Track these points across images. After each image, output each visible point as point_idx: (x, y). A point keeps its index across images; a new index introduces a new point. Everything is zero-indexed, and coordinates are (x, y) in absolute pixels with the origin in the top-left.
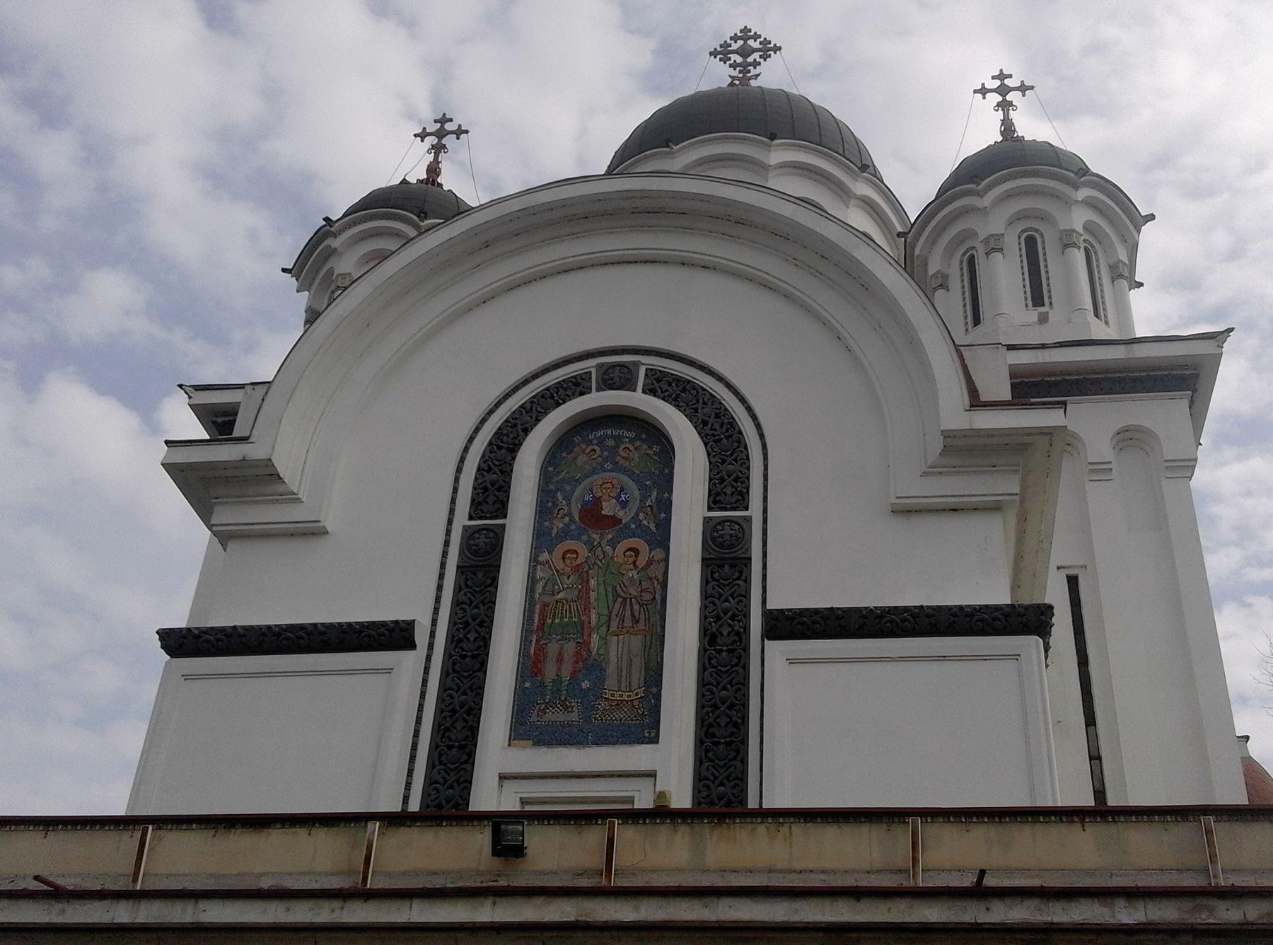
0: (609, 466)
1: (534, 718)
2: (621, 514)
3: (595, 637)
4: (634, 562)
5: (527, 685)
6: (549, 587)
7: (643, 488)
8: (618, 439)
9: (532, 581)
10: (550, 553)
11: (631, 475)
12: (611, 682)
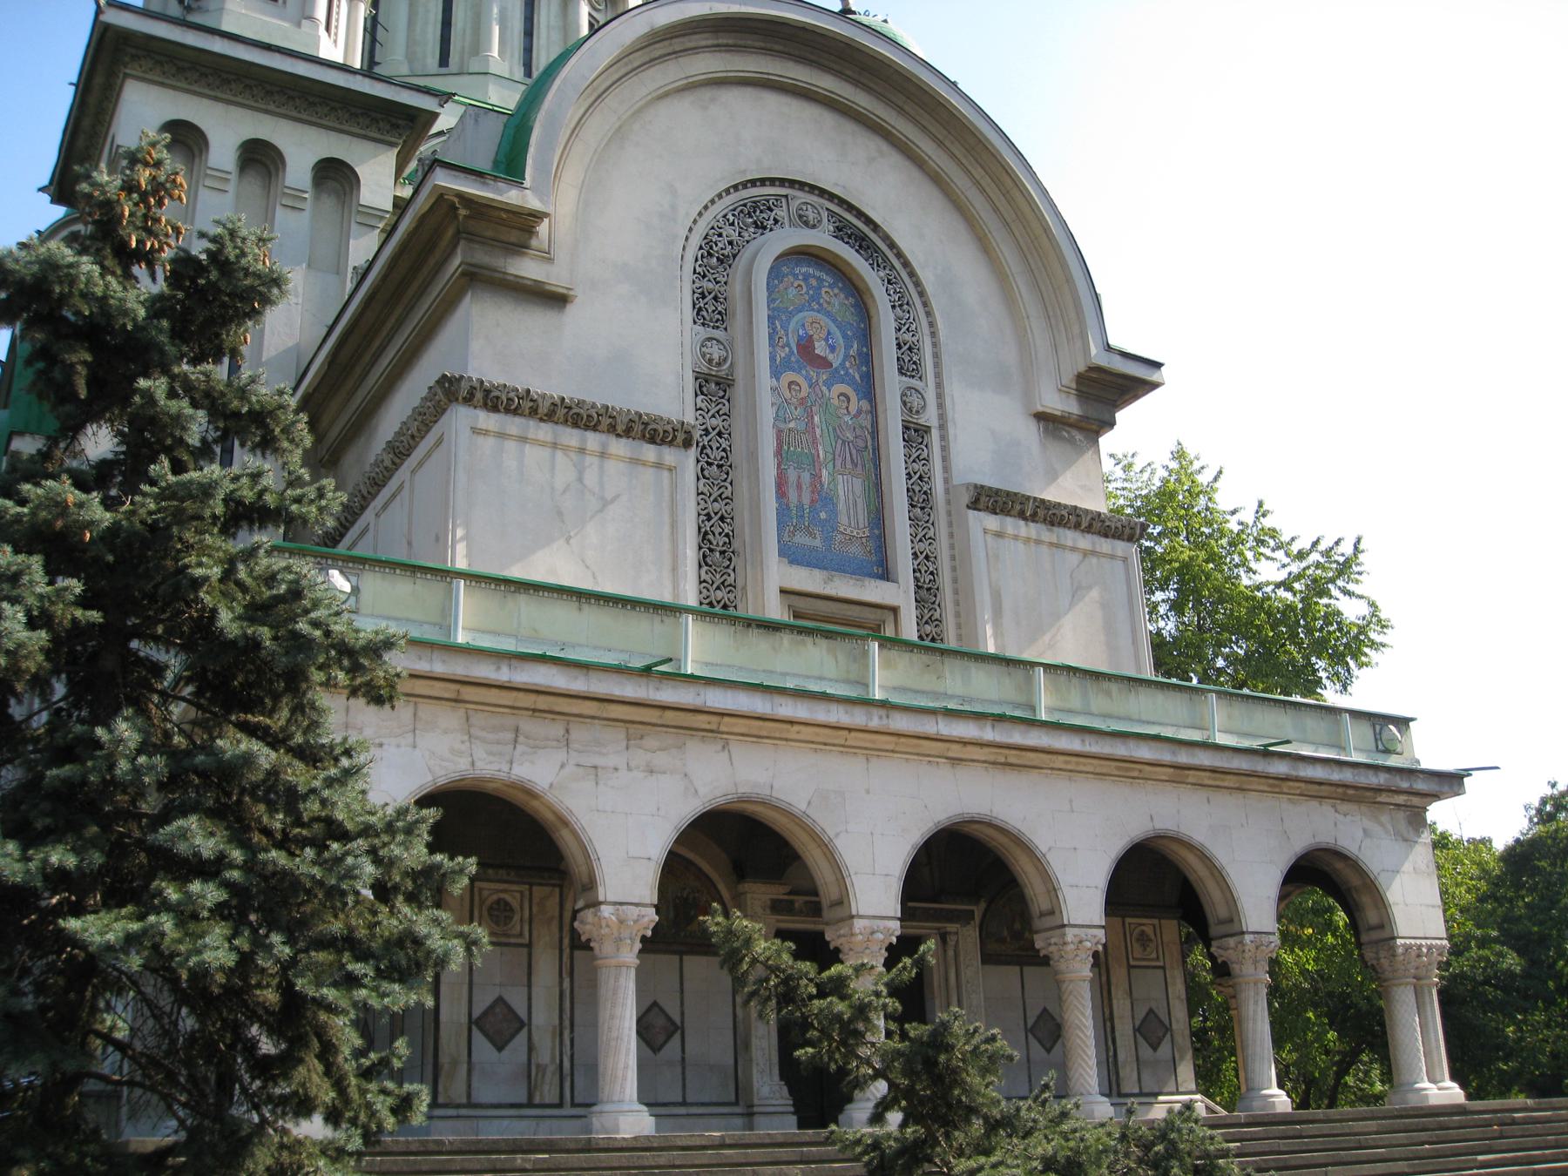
2: (830, 357)
3: (824, 473)
7: (845, 336)
11: (835, 321)
12: (843, 519)
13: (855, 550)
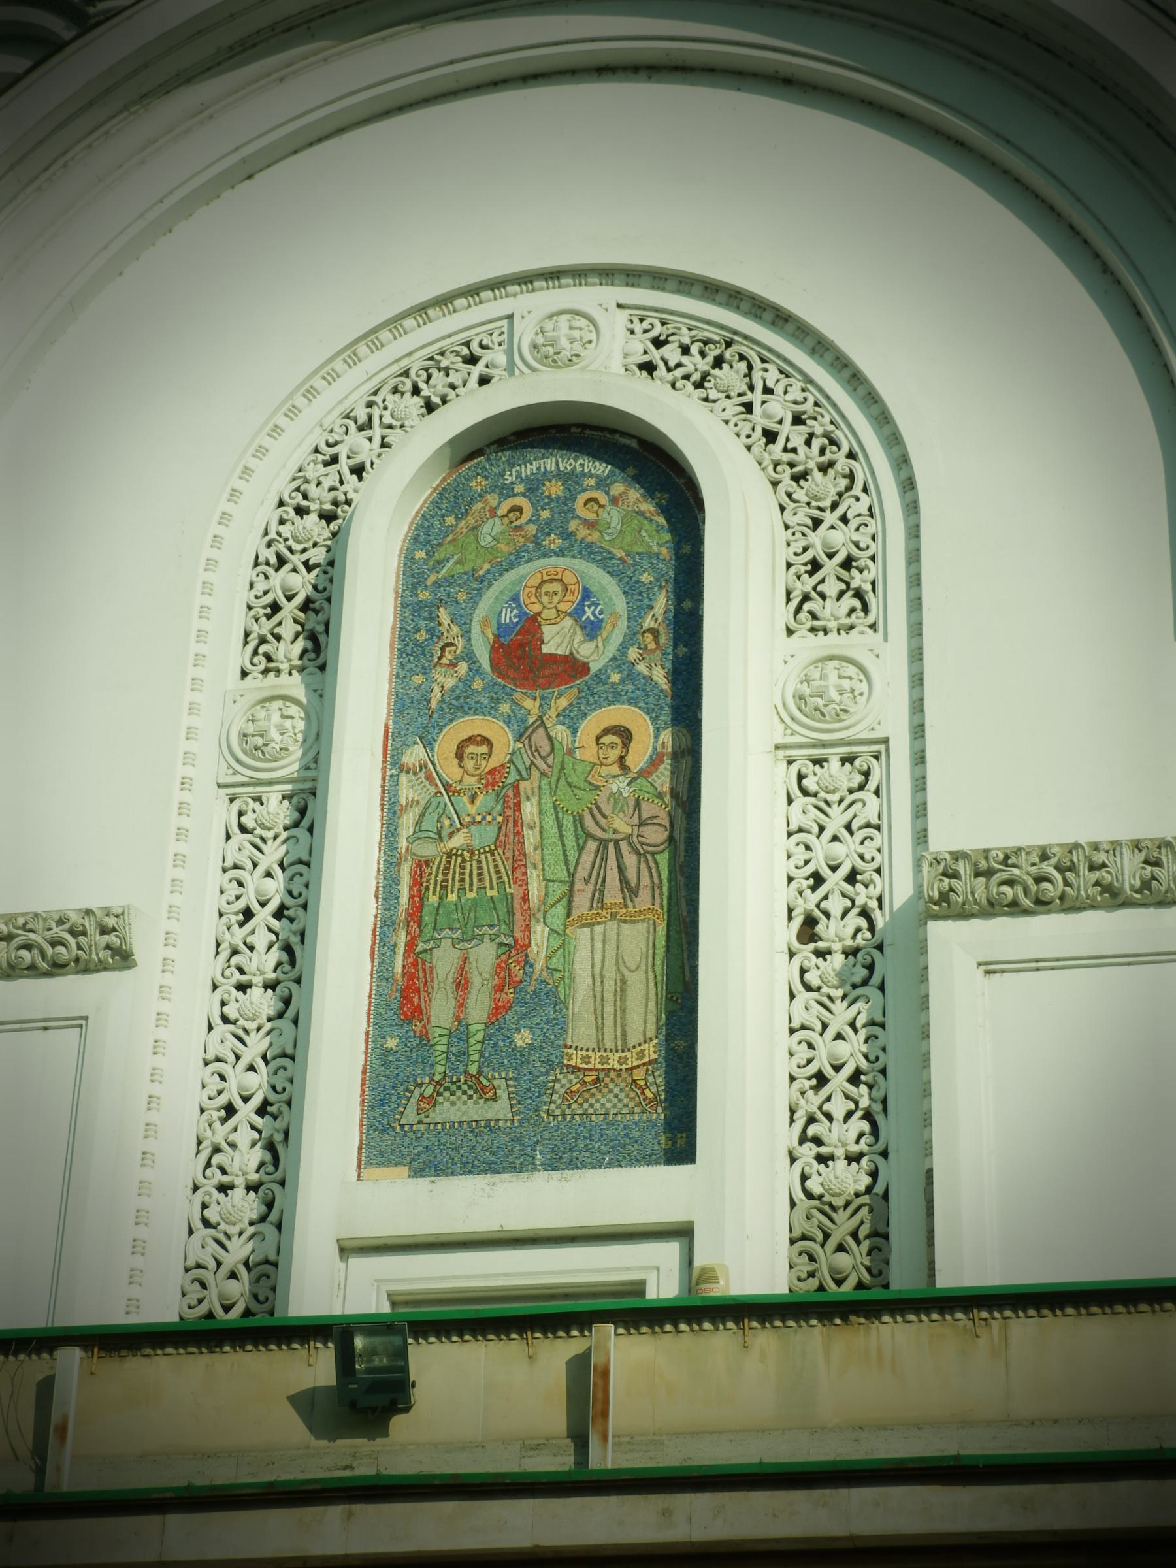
0: (554, 542)
1: (411, 1116)
2: (585, 651)
3: (539, 932)
4: (621, 759)
5: (391, 1043)
6: (430, 823)
7: (632, 589)
8: (572, 480)
9: (392, 810)
10: (428, 744)
11: (604, 560)
12: (582, 1033)
13: (610, 1103)
